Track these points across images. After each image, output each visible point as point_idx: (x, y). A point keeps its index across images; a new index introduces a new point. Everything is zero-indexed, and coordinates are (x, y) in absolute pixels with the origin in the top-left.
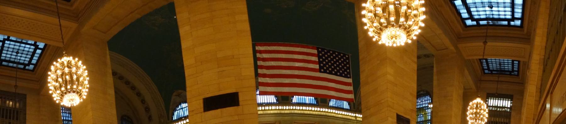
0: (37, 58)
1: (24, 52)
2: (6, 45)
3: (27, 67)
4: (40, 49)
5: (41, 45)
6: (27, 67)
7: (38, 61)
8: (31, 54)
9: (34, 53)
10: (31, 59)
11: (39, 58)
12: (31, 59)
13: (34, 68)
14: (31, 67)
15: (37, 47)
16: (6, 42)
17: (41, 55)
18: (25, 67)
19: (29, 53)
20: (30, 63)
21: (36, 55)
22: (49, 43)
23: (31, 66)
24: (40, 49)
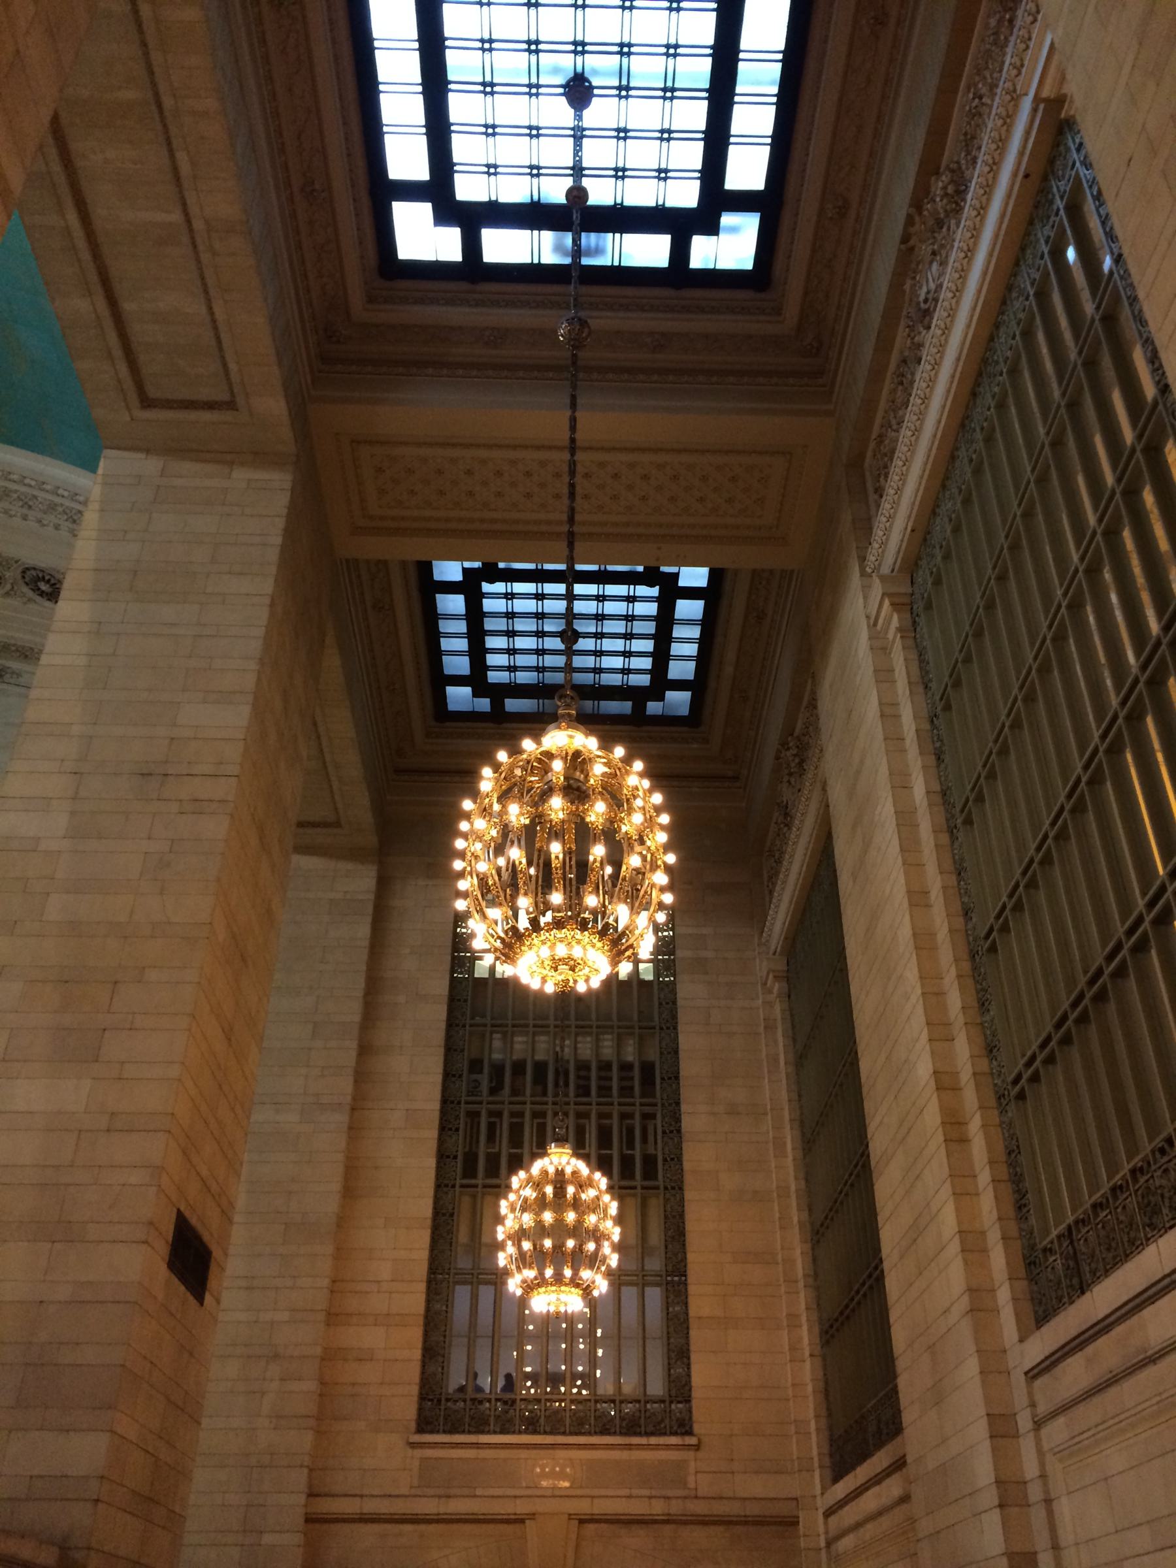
0: (692, 649)
1: (610, 627)
2: (488, 605)
3: (653, 707)
4: (691, 593)
5: (694, 576)
6: (653, 707)
7: (703, 659)
8: (650, 628)
9: (665, 620)
10: (661, 656)
11: (706, 643)
12: (661, 656)
13: (695, 704)
14: (679, 700)
15: (671, 592)
16: (486, 587)
17: (708, 623)
18: (639, 707)
19: (639, 627)
20: (660, 682)
21: (678, 632)
22: (728, 558)
23: (671, 695)
24: (691, 593)
